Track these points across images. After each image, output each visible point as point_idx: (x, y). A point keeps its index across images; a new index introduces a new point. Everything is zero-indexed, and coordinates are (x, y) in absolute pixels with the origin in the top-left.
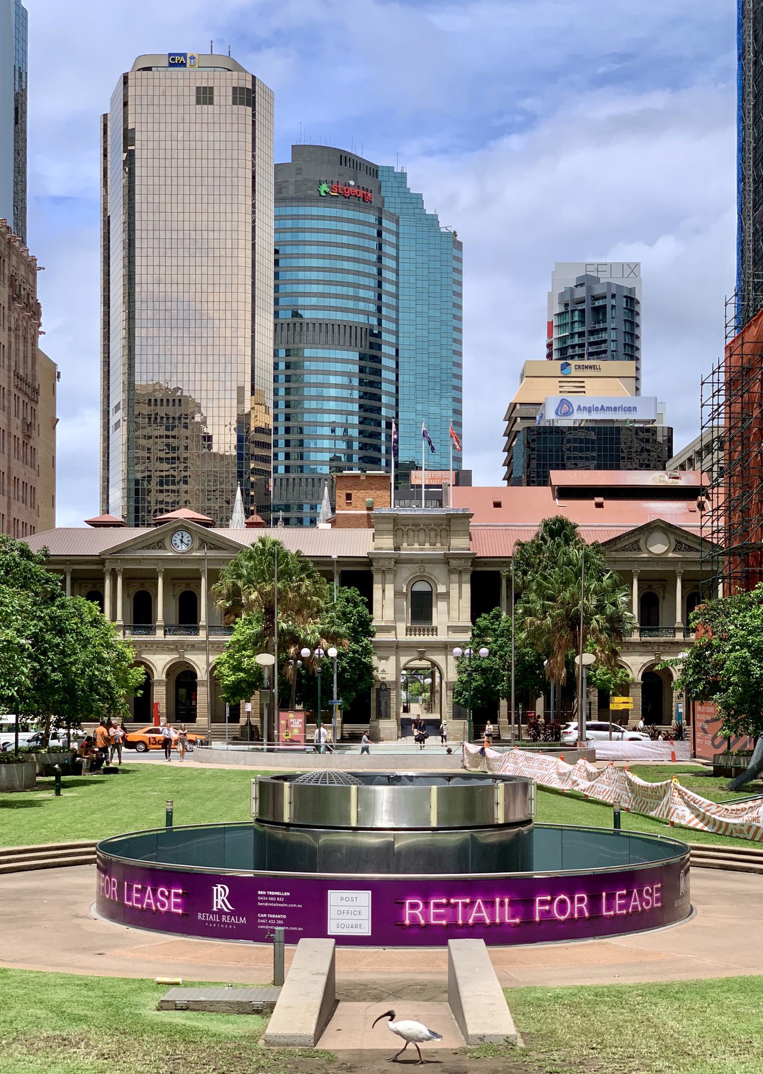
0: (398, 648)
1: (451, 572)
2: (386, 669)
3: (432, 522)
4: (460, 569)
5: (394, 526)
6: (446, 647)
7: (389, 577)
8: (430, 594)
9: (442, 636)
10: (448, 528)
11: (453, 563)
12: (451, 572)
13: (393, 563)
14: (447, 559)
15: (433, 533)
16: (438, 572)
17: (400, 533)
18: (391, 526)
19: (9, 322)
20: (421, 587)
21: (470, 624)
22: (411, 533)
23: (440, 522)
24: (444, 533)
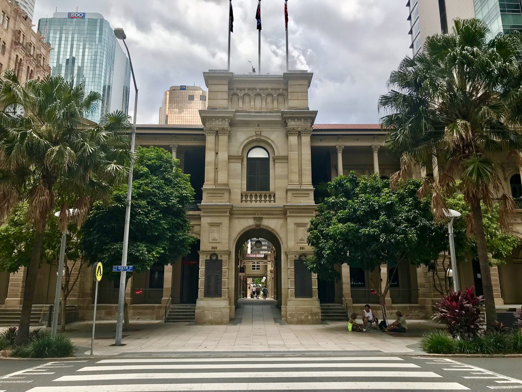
0: (232, 213)
1: (288, 134)
2: (215, 235)
3: (269, 86)
4: (300, 129)
5: (229, 89)
6: (284, 213)
7: (223, 139)
8: (266, 160)
9: (280, 202)
10: (285, 93)
11: (292, 124)
12: (288, 134)
13: (227, 123)
14: (285, 120)
15: (269, 99)
16: (275, 137)
17: (235, 98)
18: (226, 88)
19: (10, 54)
20: (258, 153)
21: (312, 188)
22: (247, 99)
23: (276, 86)
24: (281, 99)
